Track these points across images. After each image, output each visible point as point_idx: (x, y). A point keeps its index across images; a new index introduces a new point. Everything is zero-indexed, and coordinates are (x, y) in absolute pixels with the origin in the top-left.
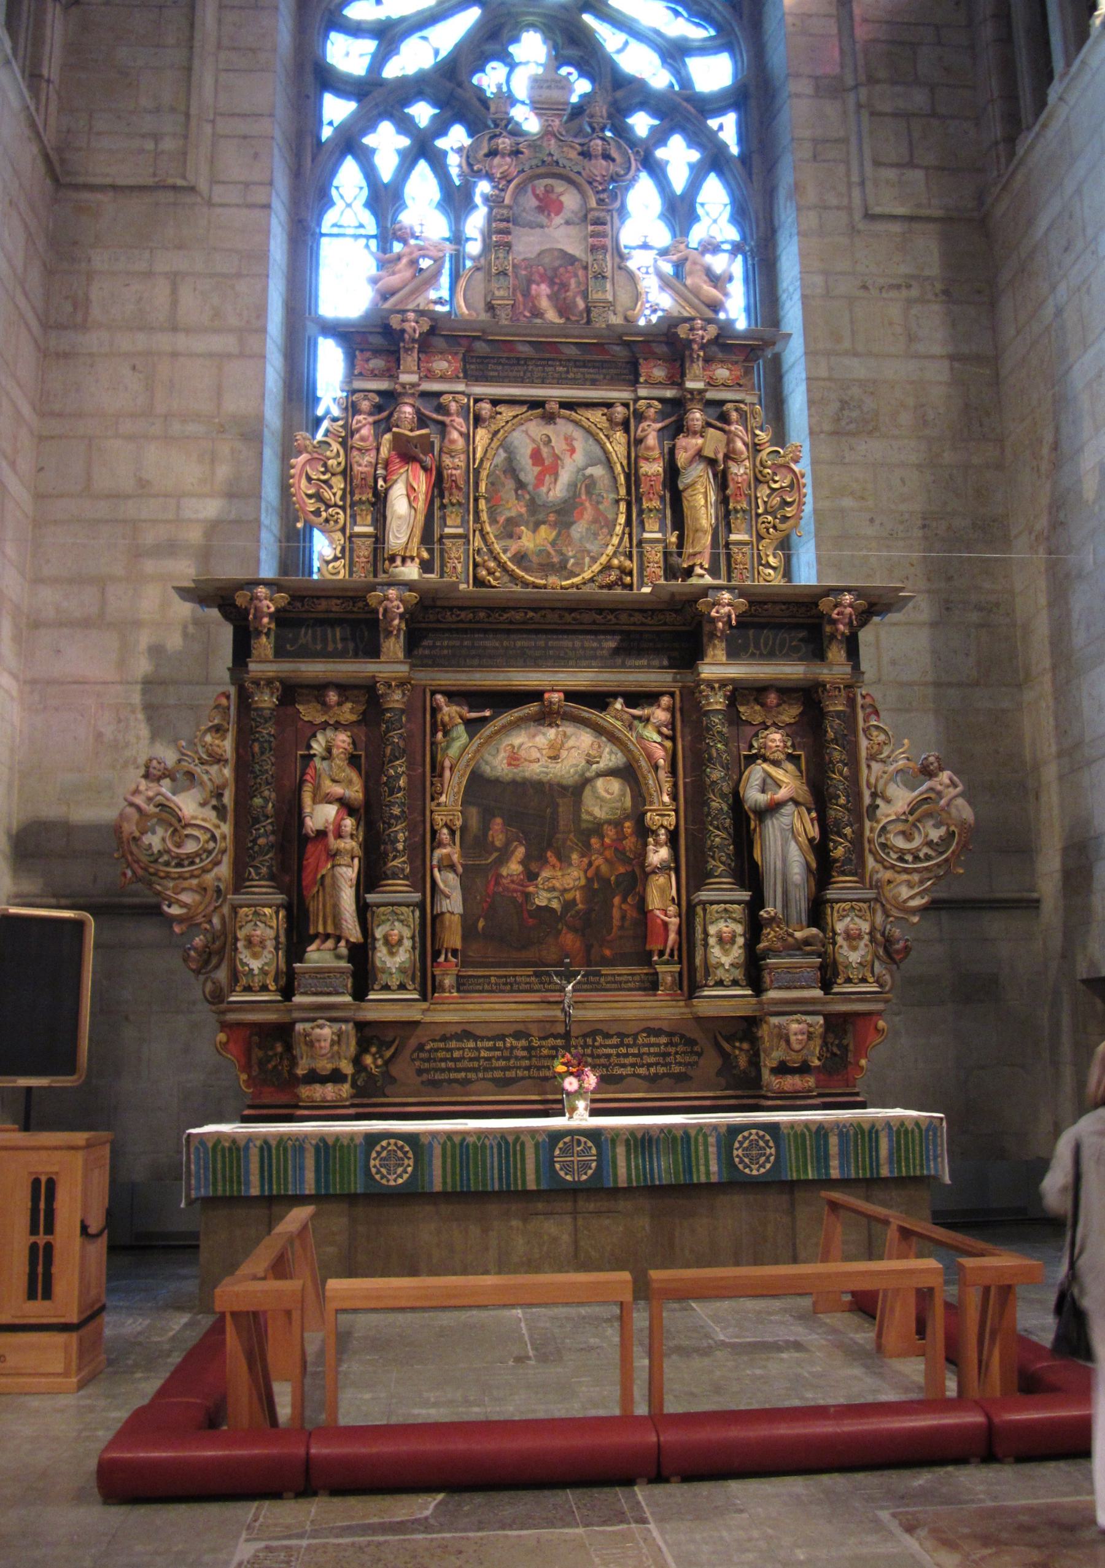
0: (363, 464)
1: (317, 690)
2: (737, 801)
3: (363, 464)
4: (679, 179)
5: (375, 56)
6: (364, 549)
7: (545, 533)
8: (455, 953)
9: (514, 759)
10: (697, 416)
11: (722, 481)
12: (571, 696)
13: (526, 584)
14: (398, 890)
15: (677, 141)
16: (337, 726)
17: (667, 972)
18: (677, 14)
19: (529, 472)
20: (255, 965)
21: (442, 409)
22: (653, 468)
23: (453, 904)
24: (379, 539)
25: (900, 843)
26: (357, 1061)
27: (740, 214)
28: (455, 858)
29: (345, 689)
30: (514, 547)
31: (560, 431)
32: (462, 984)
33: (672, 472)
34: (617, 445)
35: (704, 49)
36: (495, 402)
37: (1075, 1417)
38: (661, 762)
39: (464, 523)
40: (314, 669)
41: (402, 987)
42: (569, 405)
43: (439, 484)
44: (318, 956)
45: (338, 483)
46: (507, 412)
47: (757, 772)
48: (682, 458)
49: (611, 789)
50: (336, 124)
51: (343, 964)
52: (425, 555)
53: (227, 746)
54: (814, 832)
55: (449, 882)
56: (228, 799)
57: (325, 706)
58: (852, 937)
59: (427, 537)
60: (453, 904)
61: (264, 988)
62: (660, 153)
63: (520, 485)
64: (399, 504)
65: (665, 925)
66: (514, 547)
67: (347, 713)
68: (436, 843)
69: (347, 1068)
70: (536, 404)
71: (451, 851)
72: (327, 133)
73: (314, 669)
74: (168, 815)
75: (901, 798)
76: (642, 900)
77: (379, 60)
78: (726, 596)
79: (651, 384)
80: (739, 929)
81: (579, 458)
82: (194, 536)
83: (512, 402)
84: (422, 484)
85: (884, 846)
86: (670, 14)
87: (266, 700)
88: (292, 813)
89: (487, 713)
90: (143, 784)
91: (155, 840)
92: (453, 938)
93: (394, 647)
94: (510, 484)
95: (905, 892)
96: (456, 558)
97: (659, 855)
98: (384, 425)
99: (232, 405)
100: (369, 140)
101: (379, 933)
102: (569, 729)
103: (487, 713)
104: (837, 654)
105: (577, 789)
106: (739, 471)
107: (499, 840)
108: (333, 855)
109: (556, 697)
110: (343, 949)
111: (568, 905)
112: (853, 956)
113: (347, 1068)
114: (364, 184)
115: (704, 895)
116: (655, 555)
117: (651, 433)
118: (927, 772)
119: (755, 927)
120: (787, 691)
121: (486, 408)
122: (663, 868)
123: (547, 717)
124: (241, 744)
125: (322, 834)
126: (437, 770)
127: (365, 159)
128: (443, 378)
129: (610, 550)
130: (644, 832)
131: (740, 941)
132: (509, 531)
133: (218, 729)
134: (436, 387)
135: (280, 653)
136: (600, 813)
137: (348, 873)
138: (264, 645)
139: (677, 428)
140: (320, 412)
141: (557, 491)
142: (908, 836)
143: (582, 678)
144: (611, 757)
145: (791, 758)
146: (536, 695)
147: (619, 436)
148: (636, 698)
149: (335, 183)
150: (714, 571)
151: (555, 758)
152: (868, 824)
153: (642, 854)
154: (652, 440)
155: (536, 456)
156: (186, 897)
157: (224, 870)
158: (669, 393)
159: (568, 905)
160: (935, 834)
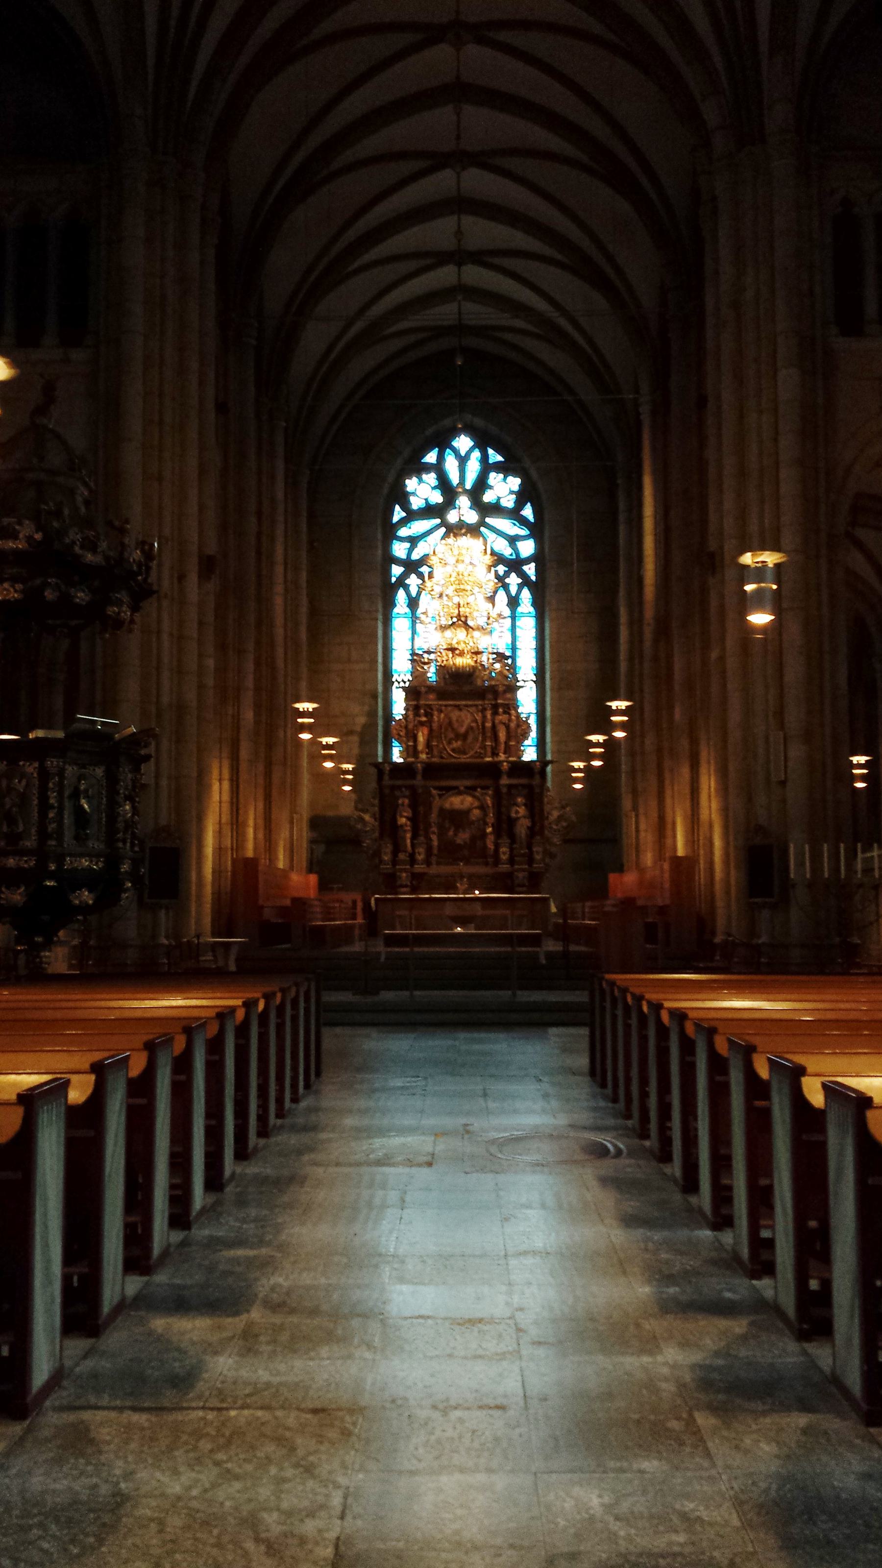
0: (410, 726)
1: (399, 787)
2: (509, 817)
3: (410, 726)
4: (513, 590)
5: (409, 549)
6: (411, 750)
7: (459, 743)
8: (435, 855)
9: (451, 804)
10: (501, 710)
11: (508, 727)
12: (466, 788)
13: (455, 758)
14: (422, 839)
15: (513, 575)
16: (405, 797)
17: (490, 860)
18: (515, 524)
19: (456, 725)
20: (386, 858)
21: (432, 709)
22: (488, 725)
23: (435, 843)
24: (415, 747)
25: (554, 827)
26: (411, 882)
27: (535, 604)
28: (436, 831)
29: (406, 787)
30: (451, 746)
31: (463, 714)
32: (438, 864)
33: (494, 727)
34: (479, 717)
35: (524, 538)
36: (446, 706)
37: (526, 933)
38: (490, 805)
39: (438, 742)
40: (399, 782)
41: (422, 864)
42: (467, 706)
43: (431, 731)
44: (402, 856)
45: (404, 731)
46: (450, 708)
47: (515, 808)
48: (497, 721)
49: (476, 812)
50: (397, 576)
51: (408, 859)
52: (427, 750)
53: (376, 802)
54: (529, 824)
55: (434, 838)
56: (377, 816)
57: (402, 792)
58: (538, 853)
59: (428, 745)
60: (435, 843)
61: (388, 864)
62: (507, 580)
63: (453, 729)
64: (421, 738)
65: (490, 849)
66: (451, 746)
67: (407, 793)
68: (431, 827)
69: (409, 884)
70: (456, 706)
71: (434, 829)
72: (394, 580)
73: (399, 782)
74: (362, 820)
75: (555, 814)
76: (485, 844)
77: (410, 551)
78: (505, 764)
79: (489, 700)
80: (508, 850)
81: (469, 720)
82: (358, 728)
83: (451, 705)
84: (426, 731)
85: (551, 828)
86: (512, 525)
87: (387, 791)
88: (394, 820)
89: (444, 792)
90: (355, 812)
91: (359, 826)
92: (435, 851)
93: (419, 777)
94: (450, 729)
95: (555, 840)
96: (435, 752)
97: (489, 830)
98: (417, 714)
99: (368, 687)
100: (407, 582)
101: (417, 851)
102: (465, 796)
103: (444, 792)
104: (537, 777)
105: (468, 812)
106: (513, 725)
107: (447, 825)
108: (405, 831)
109: (462, 788)
110: (407, 854)
111: (465, 843)
112: (538, 857)
113: (409, 884)
114: (407, 598)
115: (499, 841)
116: (489, 750)
117: (489, 714)
118: (563, 807)
119: (512, 850)
120: (523, 786)
121: (443, 708)
122: (491, 833)
123: (460, 793)
124: (382, 801)
125: (402, 826)
126: (430, 808)
127: (406, 588)
128: (432, 700)
129: (477, 747)
130: (486, 824)
131: (508, 853)
132: (449, 743)
133: (374, 798)
134: (430, 703)
135: (391, 778)
136: (474, 819)
137: (409, 835)
138: (386, 777)
139: (495, 713)
140: (394, 680)
141: (462, 730)
142: (557, 825)
143: (468, 783)
144: (476, 804)
145: (525, 805)
146: (456, 788)
147: (480, 714)
148: (485, 788)
149: (396, 598)
150: (505, 753)
151: (462, 804)
152: (546, 821)
153: (485, 830)
154: (489, 717)
155: (457, 721)
156: (368, 841)
157: (377, 834)
158: (493, 702)
159: (465, 843)
160: (565, 824)
